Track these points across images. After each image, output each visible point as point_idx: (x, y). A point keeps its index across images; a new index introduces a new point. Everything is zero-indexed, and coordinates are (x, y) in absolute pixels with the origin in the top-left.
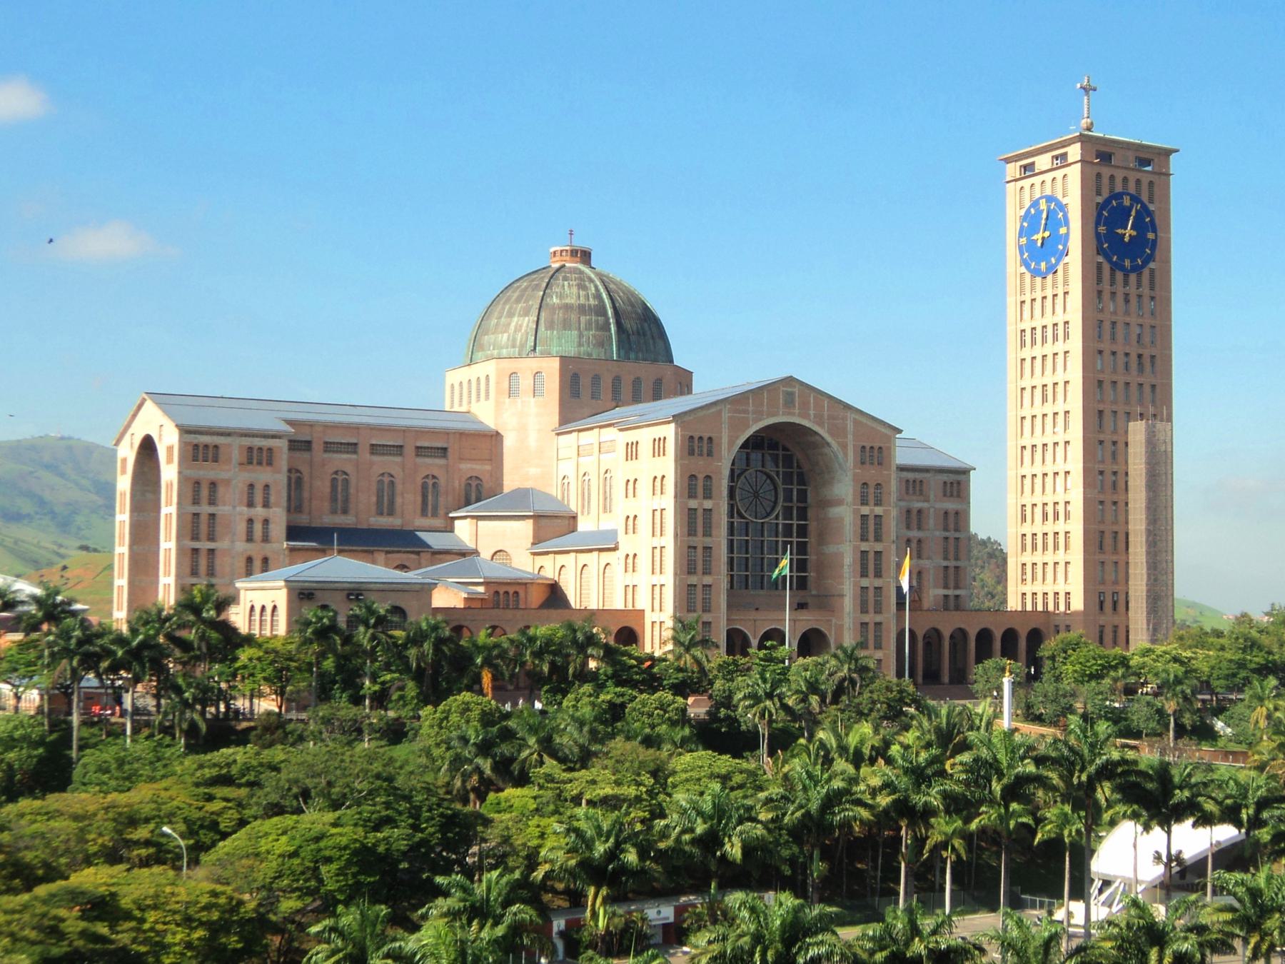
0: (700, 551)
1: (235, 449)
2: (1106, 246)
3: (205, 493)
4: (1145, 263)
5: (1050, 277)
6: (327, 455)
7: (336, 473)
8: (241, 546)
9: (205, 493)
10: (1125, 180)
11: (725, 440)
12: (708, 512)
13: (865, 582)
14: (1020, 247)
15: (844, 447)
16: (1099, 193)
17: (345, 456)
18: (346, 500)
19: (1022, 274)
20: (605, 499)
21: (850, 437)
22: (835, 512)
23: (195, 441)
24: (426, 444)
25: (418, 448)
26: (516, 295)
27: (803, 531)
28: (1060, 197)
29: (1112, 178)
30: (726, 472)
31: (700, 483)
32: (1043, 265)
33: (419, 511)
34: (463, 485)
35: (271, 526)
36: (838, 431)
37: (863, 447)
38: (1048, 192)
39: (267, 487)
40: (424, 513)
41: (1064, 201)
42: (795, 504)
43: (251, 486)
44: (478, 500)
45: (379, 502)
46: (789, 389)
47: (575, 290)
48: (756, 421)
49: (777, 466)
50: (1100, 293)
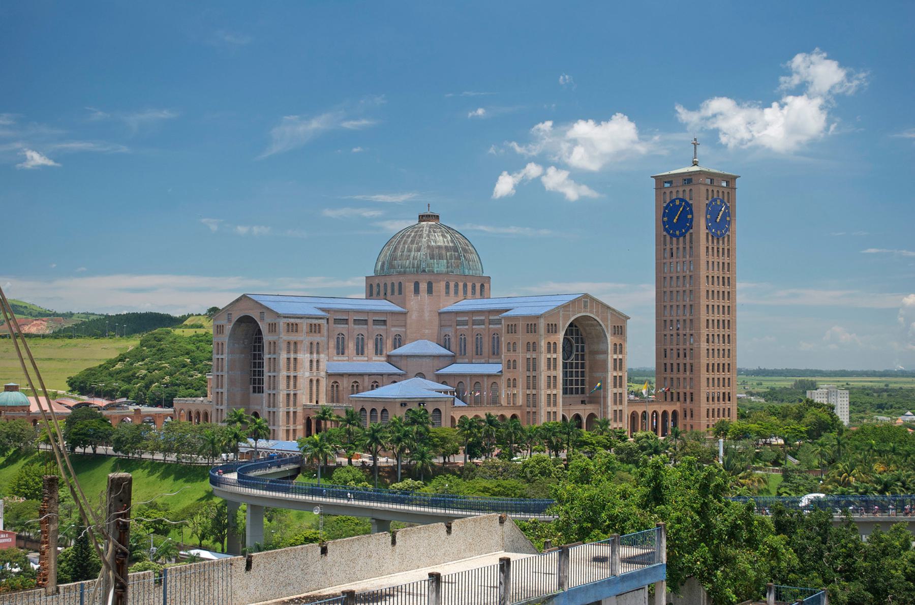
0: (552, 378)
1: (304, 325)
2: (710, 224)
3: (292, 347)
4: (726, 232)
5: (681, 239)
6: (334, 326)
7: (339, 335)
8: (307, 374)
9: (292, 347)
10: (718, 191)
11: (561, 325)
12: (555, 359)
13: (615, 390)
14: (664, 222)
15: (607, 326)
16: (707, 199)
17: (343, 326)
18: (343, 349)
19: (665, 236)
20: (477, 348)
21: (609, 322)
22: (601, 357)
23: (288, 322)
24: (377, 319)
25: (374, 320)
26: (410, 240)
27: (583, 366)
28: (688, 200)
29: (713, 191)
30: (562, 340)
31: (552, 346)
32: (677, 233)
33: (374, 352)
34: (393, 338)
35: (321, 364)
36: (605, 319)
37: (614, 326)
38: (681, 196)
39: (318, 343)
40: (376, 354)
41: (691, 202)
42: (580, 353)
43: (311, 343)
44: (400, 346)
45: (357, 349)
46: (586, 300)
47: (441, 238)
48: (573, 315)
49: (572, 335)
50: (707, 248)
